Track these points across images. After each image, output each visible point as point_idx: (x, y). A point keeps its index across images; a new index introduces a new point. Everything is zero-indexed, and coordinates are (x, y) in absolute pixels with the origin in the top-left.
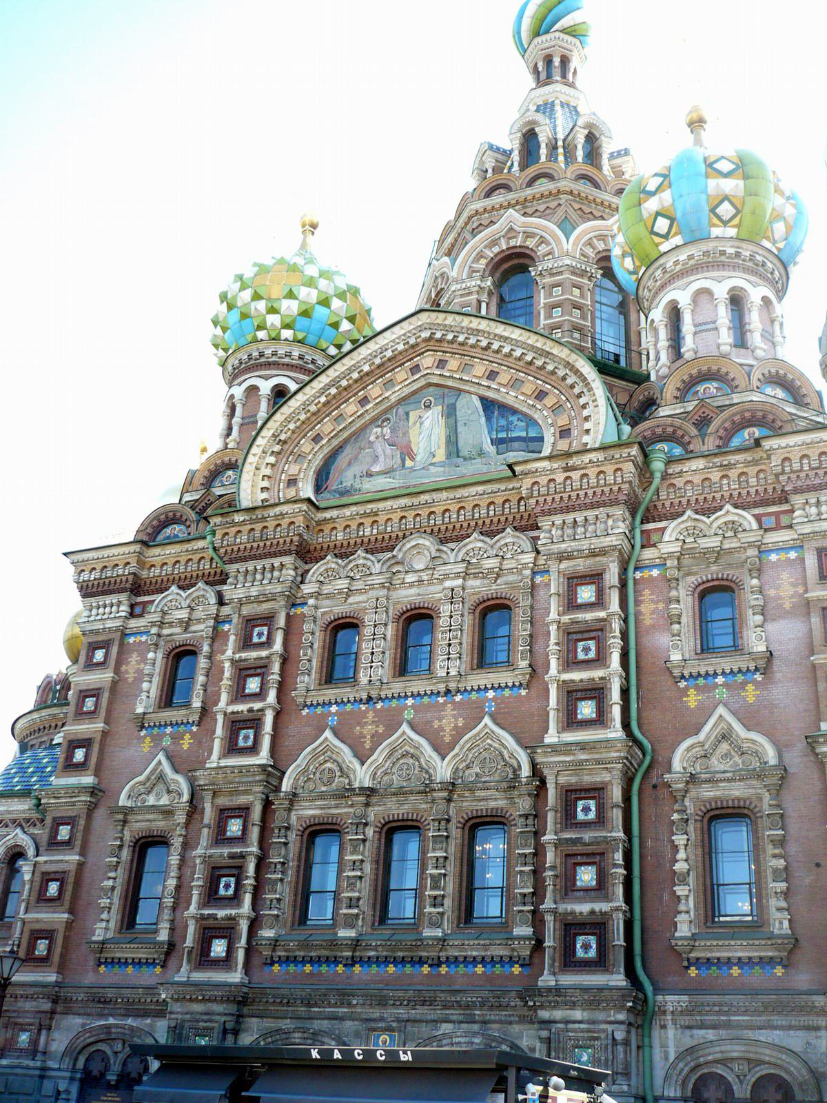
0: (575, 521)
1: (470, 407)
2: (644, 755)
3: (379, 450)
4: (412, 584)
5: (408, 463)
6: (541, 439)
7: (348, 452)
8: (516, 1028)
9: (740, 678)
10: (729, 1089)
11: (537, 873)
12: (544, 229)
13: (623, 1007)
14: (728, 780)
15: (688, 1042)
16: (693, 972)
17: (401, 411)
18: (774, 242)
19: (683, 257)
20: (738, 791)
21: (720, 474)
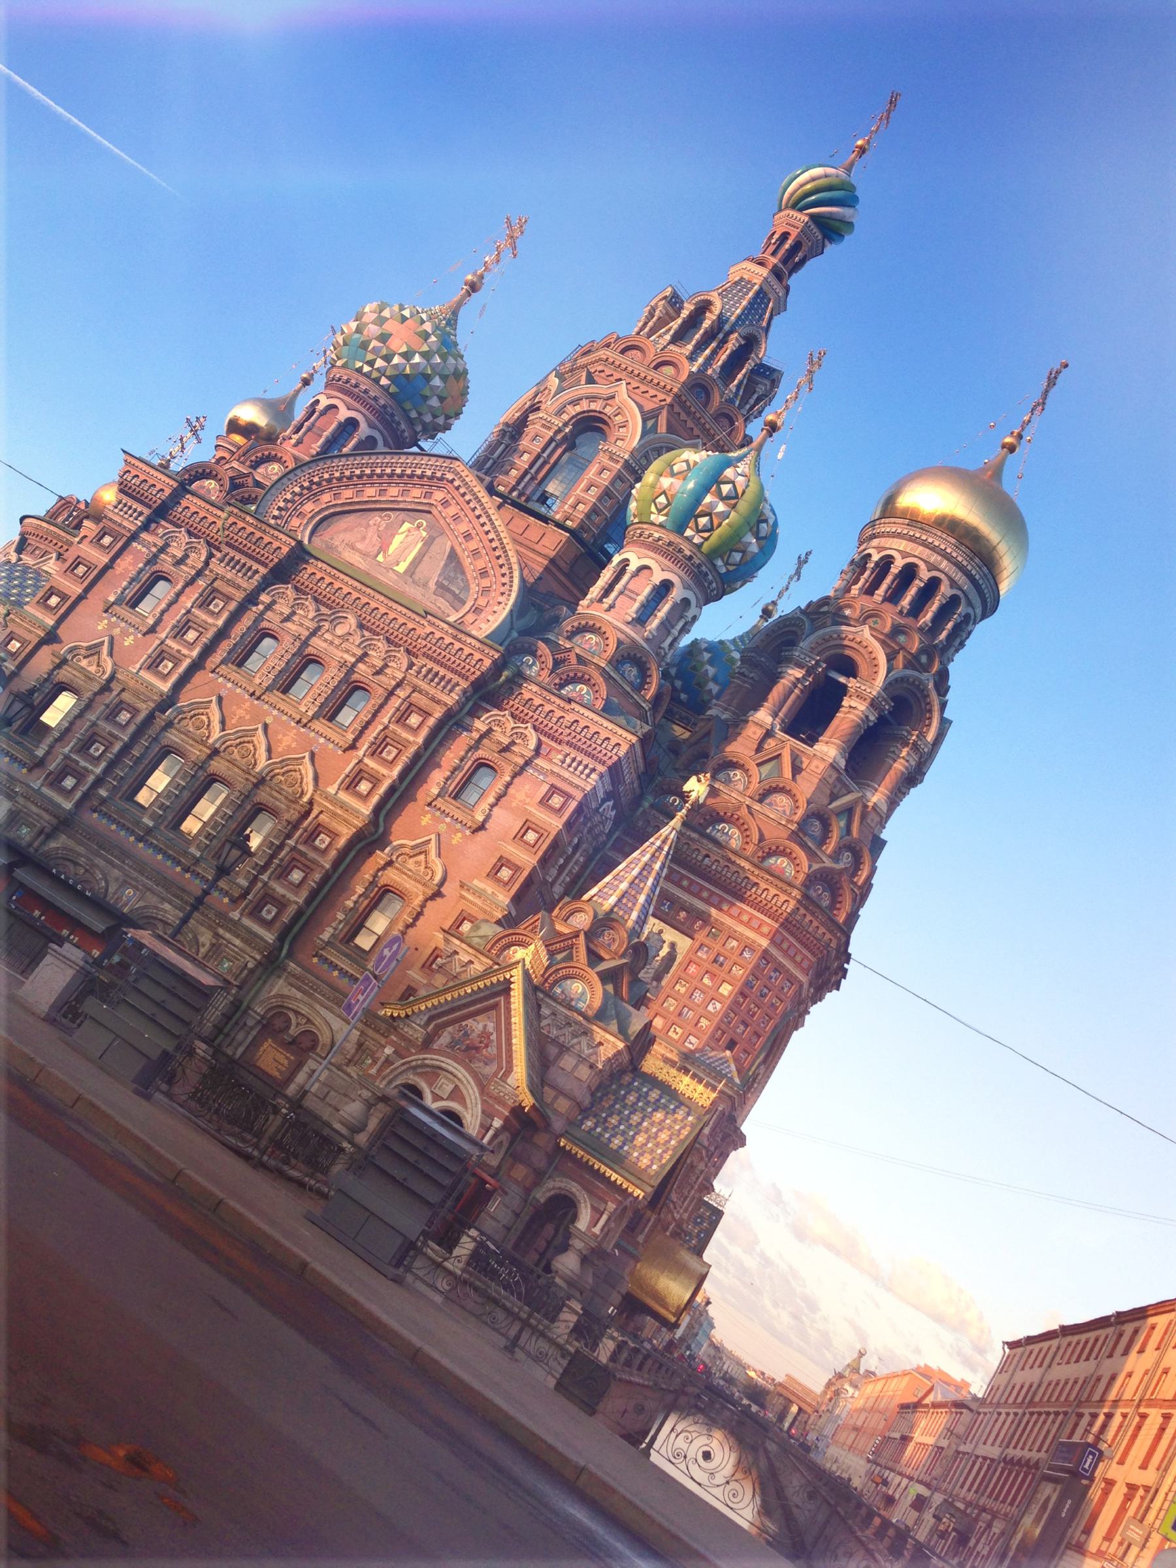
0: (437, 674)
1: (444, 545)
2: (376, 831)
3: (370, 534)
4: (326, 641)
5: (380, 558)
6: (464, 603)
7: (351, 518)
8: (203, 929)
9: (458, 826)
10: (288, 1027)
11: (272, 857)
12: (633, 417)
13: (261, 953)
14: (409, 877)
15: (285, 991)
16: (315, 960)
17: (403, 515)
18: (727, 564)
19: (656, 535)
20: (408, 885)
21: (541, 702)
